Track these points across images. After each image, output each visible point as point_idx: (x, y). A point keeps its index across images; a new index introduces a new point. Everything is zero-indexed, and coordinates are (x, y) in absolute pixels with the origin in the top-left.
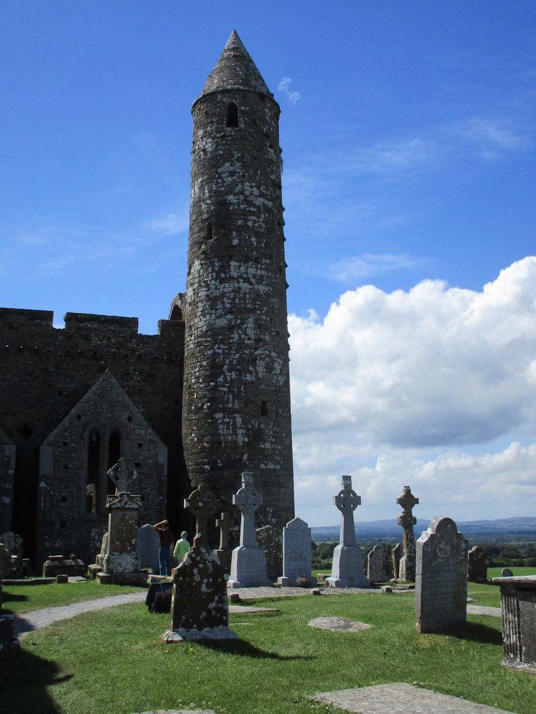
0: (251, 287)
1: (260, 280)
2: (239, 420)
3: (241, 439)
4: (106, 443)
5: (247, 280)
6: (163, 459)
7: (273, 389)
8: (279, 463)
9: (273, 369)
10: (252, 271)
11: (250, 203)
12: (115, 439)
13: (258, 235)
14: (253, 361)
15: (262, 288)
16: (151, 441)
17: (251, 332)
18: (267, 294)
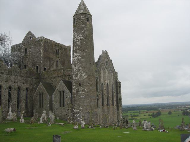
0: (76, 58)
1: (79, 56)
2: (75, 88)
3: (75, 92)
4: (62, 94)
5: (76, 57)
6: (71, 96)
7: (82, 80)
8: (83, 96)
9: (82, 75)
10: (77, 54)
11: (77, 39)
12: (64, 93)
13: (78, 46)
14: (77, 74)
15: (79, 58)
16: (69, 93)
17: (77, 68)
18: (81, 59)
